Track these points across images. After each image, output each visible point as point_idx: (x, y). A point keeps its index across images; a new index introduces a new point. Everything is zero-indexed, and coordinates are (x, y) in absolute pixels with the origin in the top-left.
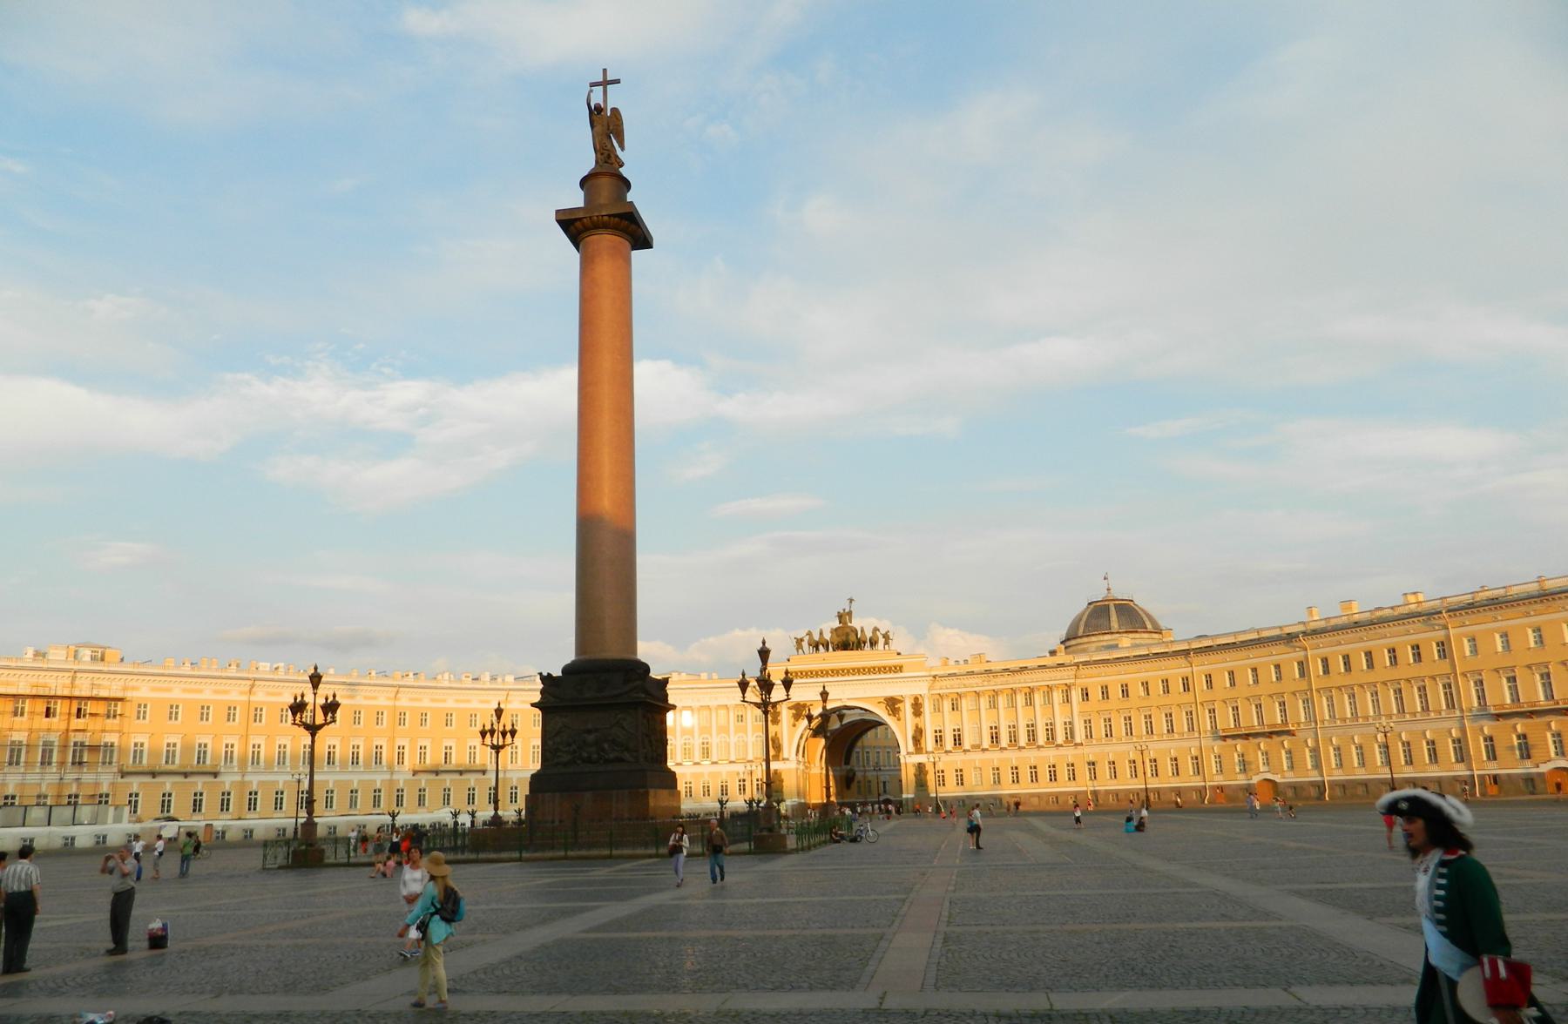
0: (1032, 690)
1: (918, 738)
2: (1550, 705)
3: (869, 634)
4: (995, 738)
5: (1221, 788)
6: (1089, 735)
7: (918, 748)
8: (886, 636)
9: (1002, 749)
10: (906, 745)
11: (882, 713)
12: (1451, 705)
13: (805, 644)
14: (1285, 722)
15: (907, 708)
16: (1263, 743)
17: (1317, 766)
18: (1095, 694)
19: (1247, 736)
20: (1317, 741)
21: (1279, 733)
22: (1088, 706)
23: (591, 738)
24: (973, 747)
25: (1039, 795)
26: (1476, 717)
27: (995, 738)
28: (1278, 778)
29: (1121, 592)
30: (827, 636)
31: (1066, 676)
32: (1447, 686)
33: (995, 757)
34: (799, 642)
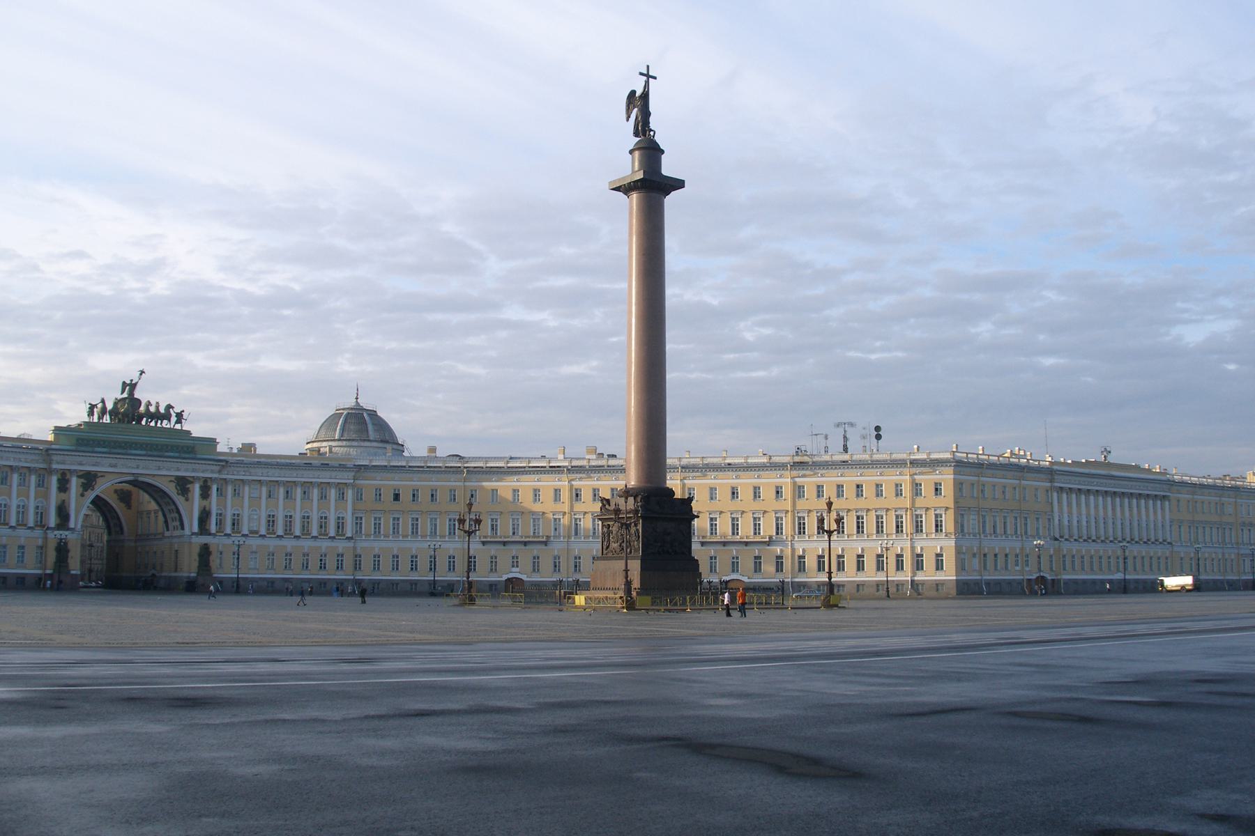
1: (204, 516)
2: (737, 538)
3: (162, 410)
4: (271, 521)
6: (358, 530)
7: (203, 529)
8: (180, 416)
11: (171, 489)
15: (196, 489)
16: (514, 550)
24: (252, 532)
25: (309, 580)
27: (271, 521)
28: (524, 577)
29: (366, 403)
31: (346, 478)
33: (272, 543)
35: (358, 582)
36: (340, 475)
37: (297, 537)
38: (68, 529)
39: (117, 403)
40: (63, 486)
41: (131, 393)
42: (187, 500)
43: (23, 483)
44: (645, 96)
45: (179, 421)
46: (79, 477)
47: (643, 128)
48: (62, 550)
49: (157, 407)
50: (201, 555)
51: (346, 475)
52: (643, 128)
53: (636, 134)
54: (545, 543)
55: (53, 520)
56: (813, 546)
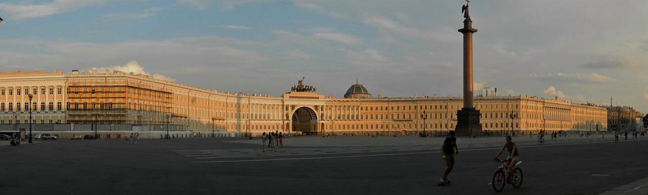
0: (349, 106)
1: (322, 115)
3: (310, 88)
4: (339, 118)
5: (393, 131)
6: (362, 118)
8: (314, 89)
10: (319, 118)
12: (446, 117)
14: (410, 118)
17: (416, 127)
18: (364, 109)
19: (400, 121)
20: (417, 122)
21: (408, 121)
22: (362, 111)
26: (450, 120)
27: (339, 118)
29: (359, 83)
30: (296, 87)
31: (358, 104)
32: (446, 114)
33: (339, 122)
41: (301, 84)
44: (467, 6)
47: (466, 15)
49: (309, 87)
52: (466, 15)
53: (465, 17)
54: (412, 121)
55: (285, 118)
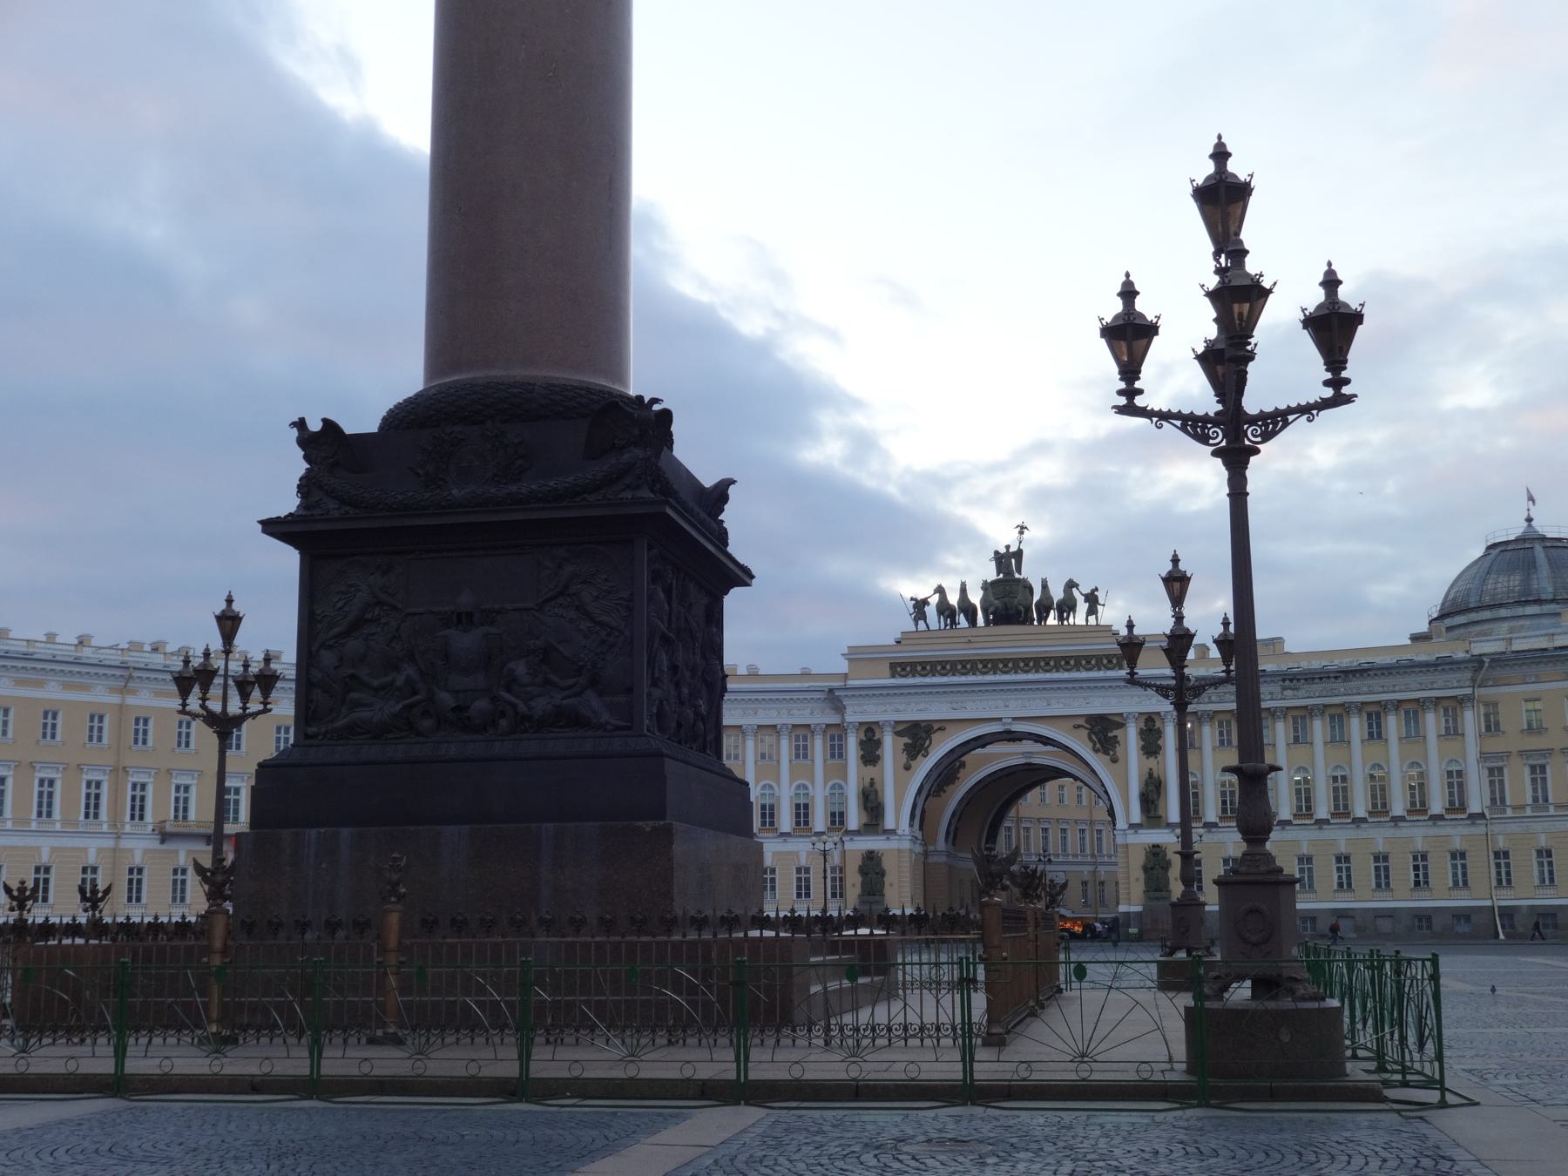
3: (1057, 594)
6: (1498, 800)
8: (1092, 600)
9: (1321, 823)
13: (931, 611)
15: (1131, 737)
23: (465, 642)
30: (976, 598)
34: (920, 605)
35: (1508, 913)
36: (1440, 678)
37: (1358, 821)
38: (886, 832)
39: (987, 586)
40: (870, 755)
41: (1009, 573)
42: (1114, 761)
43: (801, 752)
45: (1092, 611)
46: (898, 734)
48: (872, 866)
49: (1045, 586)
50: (1146, 869)
51: (1453, 677)
55: (854, 820)
56: (401, 497)
